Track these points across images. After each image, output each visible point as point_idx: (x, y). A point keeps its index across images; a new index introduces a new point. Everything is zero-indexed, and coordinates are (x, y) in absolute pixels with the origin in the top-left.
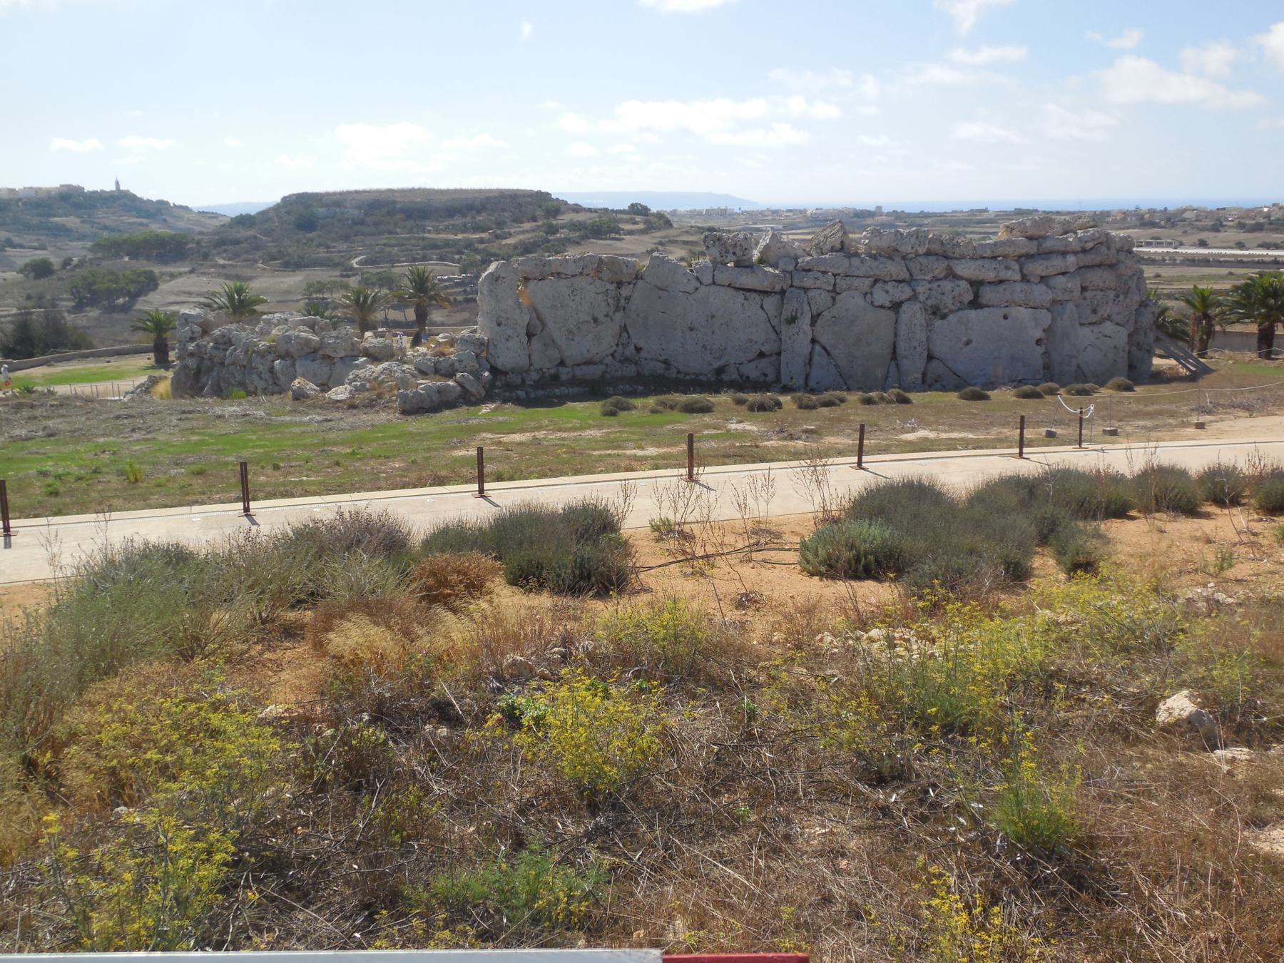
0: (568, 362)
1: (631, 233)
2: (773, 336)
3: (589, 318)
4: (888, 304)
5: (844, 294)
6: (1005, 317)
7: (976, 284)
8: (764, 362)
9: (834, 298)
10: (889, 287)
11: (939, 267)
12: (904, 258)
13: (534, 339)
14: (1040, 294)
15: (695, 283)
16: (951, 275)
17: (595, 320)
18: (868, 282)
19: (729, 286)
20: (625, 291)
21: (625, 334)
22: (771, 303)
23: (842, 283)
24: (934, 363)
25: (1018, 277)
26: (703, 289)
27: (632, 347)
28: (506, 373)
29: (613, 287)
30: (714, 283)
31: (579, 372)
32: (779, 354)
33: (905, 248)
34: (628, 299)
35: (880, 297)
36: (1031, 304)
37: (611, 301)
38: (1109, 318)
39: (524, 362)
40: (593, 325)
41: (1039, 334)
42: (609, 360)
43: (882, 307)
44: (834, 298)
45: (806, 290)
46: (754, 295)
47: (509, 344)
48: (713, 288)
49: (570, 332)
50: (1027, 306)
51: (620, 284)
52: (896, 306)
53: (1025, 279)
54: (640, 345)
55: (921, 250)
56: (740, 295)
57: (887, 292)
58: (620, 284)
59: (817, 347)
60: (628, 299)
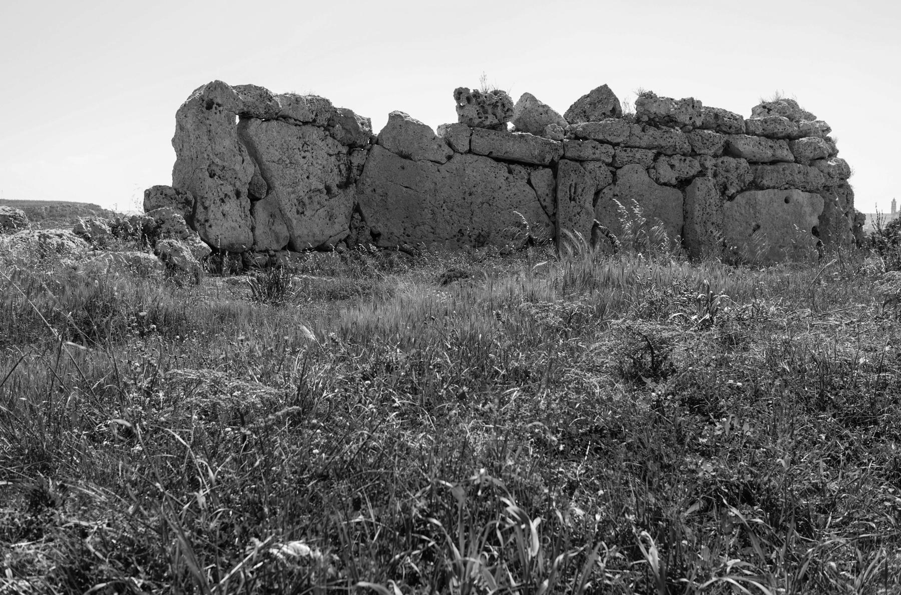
3: (321, 187)
4: (674, 182)
5: (626, 168)
6: (787, 201)
9: (614, 174)
10: (675, 161)
11: (720, 139)
13: (259, 205)
15: (447, 150)
16: (729, 150)
17: (328, 189)
18: (651, 154)
20: (357, 159)
21: (357, 215)
22: (541, 178)
23: (622, 155)
27: (367, 232)
29: (345, 150)
30: (470, 151)
34: (361, 169)
35: (666, 173)
36: (808, 188)
37: (342, 167)
40: (325, 196)
41: (815, 221)
43: (665, 184)
44: (614, 174)
45: (581, 161)
46: (517, 168)
47: (226, 208)
49: (301, 202)
50: (805, 189)
51: (352, 147)
52: (683, 184)
54: (380, 228)
55: (698, 123)
56: (503, 169)
57: (672, 166)
58: (352, 147)
60: (361, 169)
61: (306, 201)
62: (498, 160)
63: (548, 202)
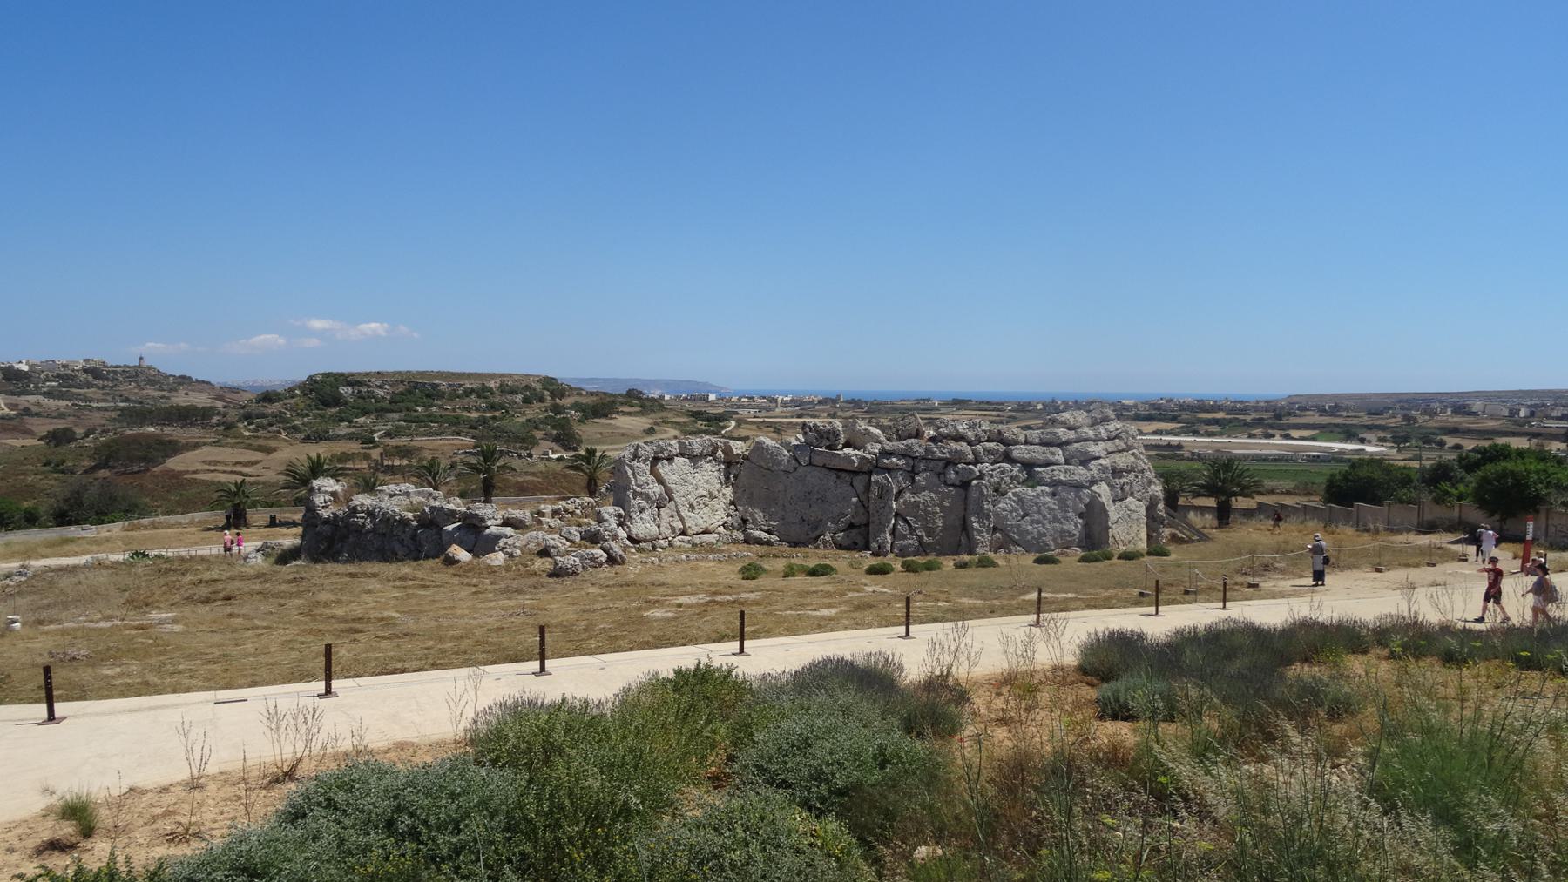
0: (690, 532)
1: (629, 414)
2: (862, 510)
6: (1054, 495)
7: (1028, 466)
8: (854, 532)
12: (970, 444)
18: (941, 464)
22: (859, 482)
31: (697, 540)
32: (867, 525)
33: (971, 435)
42: (721, 529)
63: (863, 498)
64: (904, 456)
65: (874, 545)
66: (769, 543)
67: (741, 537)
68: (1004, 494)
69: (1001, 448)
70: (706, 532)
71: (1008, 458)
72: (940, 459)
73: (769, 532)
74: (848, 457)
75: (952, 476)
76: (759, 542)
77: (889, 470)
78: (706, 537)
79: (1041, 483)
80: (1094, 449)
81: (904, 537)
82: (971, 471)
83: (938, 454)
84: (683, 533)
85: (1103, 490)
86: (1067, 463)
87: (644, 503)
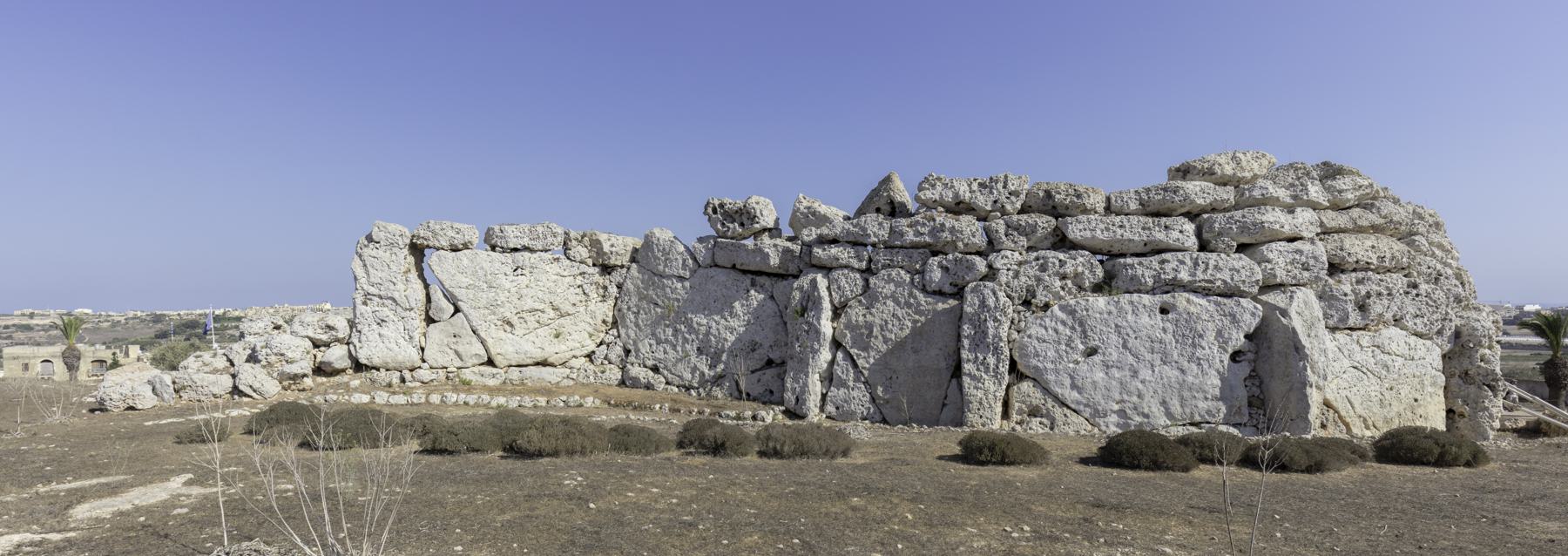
0: (498, 360)
4: (947, 289)
9: (867, 281)
14: (1231, 267)
19: (734, 267)
24: (1026, 386)
25: (1192, 242)
26: (701, 271)
28: (368, 368)
38: (1397, 321)
39: (410, 354)
47: (384, 331)
48: (713, 271)
50: (1206, 292)
53: (1203, 247)
56: (747, 280)
59: (840, 355)
61: (515, 320)
62: (745, 272)
64: (855, 244)
65: (789, 397)
66: (649, 387)
67: (615, 374)
68: (1047, 306)
69: (1045, 223)
70: (544, 363)
71: (1061, 242)
72: (915, 246)
73: (655, 369)
74: (759, 250)
75: (936, 275)
76: (636, 383)
77: (827, 269)
78: (545, 372)
79: (1135, 287)
80: (1274, 218)
81: (843, 384)
82: (971, 267)
83: (910, 236)
84: (490, 362)
85: (1303, 311)
86: (1203, 247)
87: (385, 312)
